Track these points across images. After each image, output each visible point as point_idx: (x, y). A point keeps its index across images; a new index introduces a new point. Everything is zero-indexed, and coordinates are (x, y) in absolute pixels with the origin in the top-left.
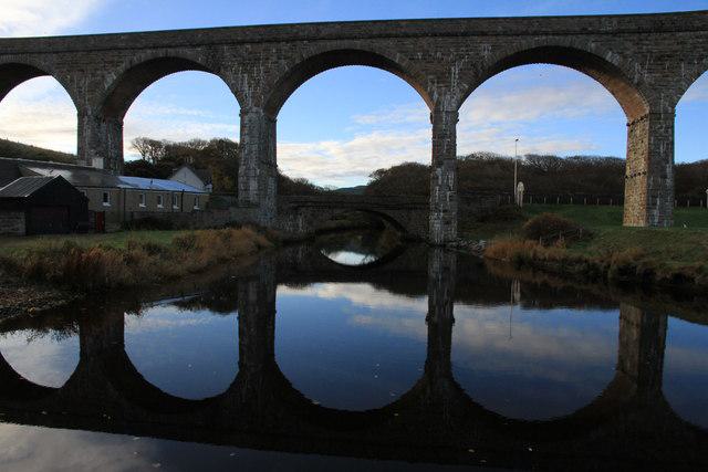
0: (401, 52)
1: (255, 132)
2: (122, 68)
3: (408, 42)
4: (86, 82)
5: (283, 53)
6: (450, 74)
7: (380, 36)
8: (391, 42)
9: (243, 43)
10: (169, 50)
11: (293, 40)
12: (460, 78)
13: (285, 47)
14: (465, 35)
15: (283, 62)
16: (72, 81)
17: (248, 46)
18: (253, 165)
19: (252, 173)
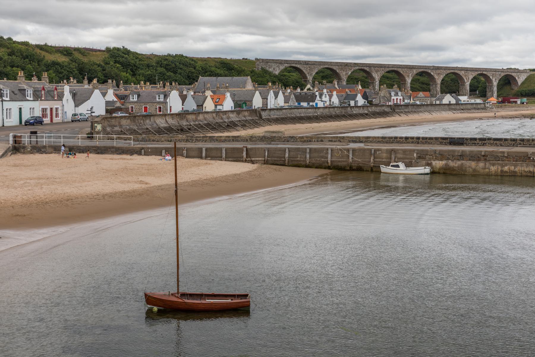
7: (399, 68)
8: (401, 69)
9: (376, 67)
13: (383, 69)
14: (412, 68)
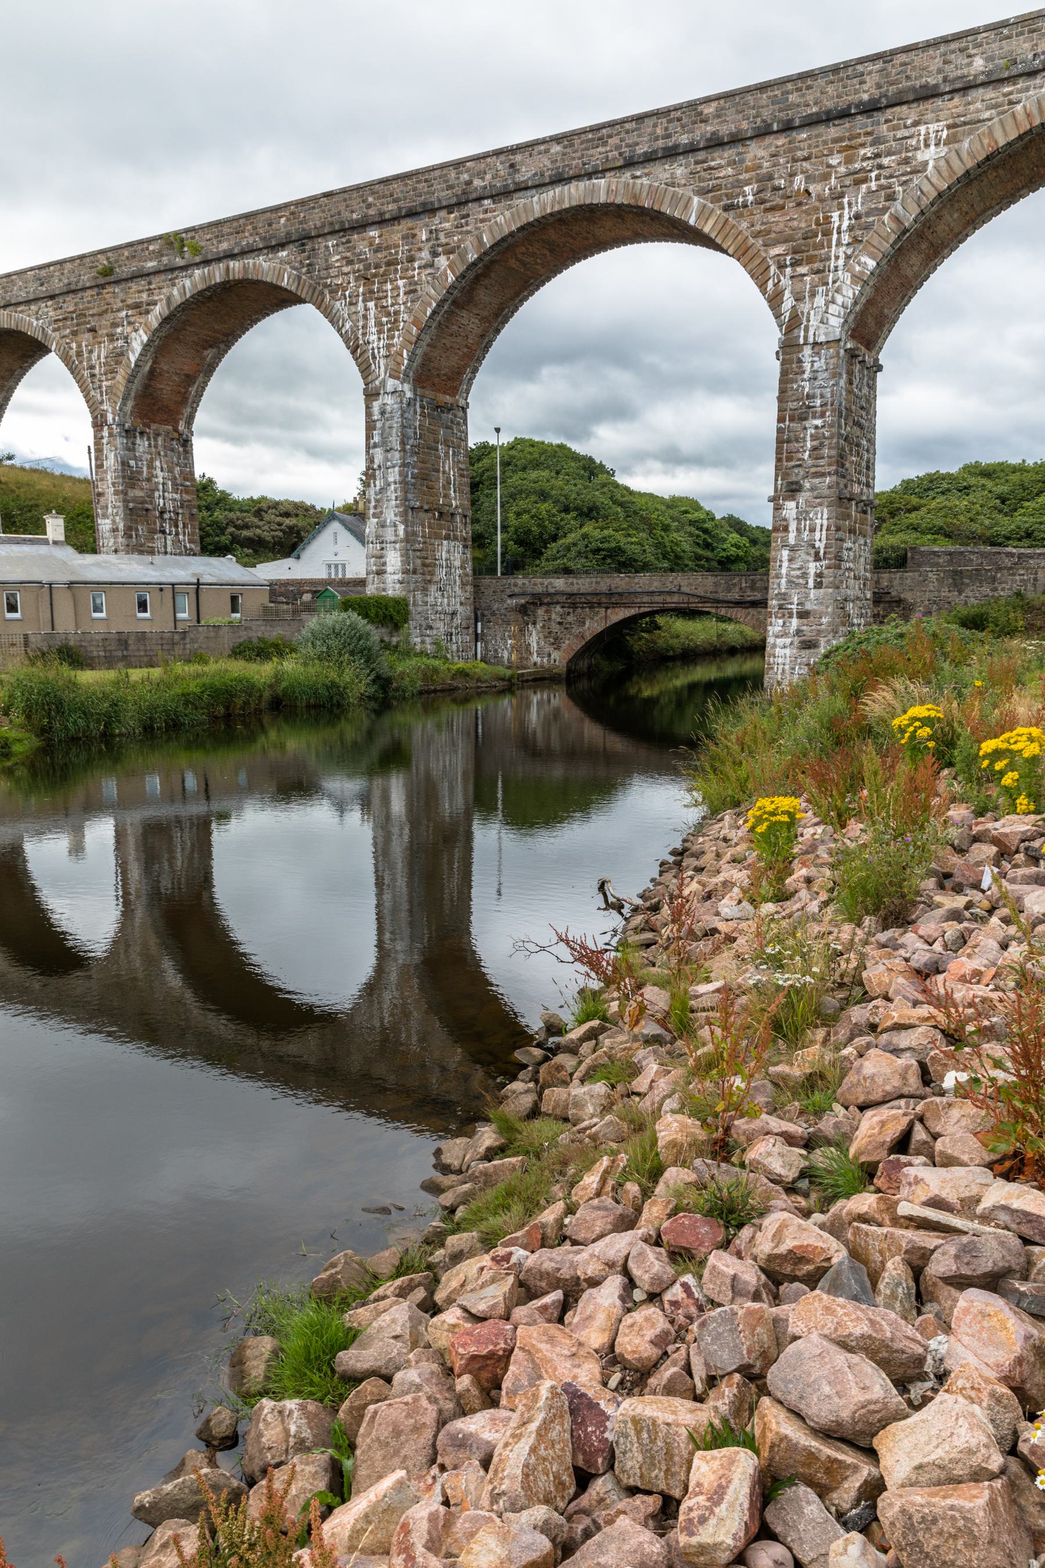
0: (702, 192)
1: (395, 442)
2: (154, 318)
3: (719, 158)
4: (101, 353)
5: (443, 239)
6: (827, 233)
7: (650, 158)
8: (679, 170)
9: (362, 226)
10: (231, 264)
11: (460, 204)
12: (856, 241)
13: (445, 222)
15: (442, 261)
16: (79, 354)
17: (373, 233)
18: (391, 514)
19: (389, 535)
